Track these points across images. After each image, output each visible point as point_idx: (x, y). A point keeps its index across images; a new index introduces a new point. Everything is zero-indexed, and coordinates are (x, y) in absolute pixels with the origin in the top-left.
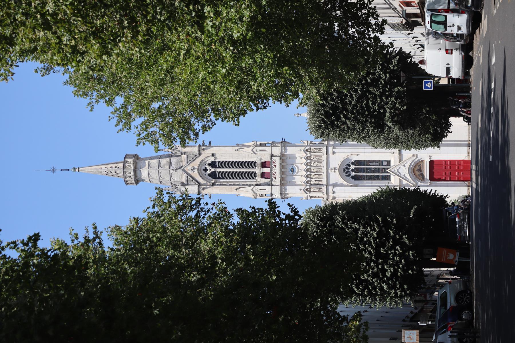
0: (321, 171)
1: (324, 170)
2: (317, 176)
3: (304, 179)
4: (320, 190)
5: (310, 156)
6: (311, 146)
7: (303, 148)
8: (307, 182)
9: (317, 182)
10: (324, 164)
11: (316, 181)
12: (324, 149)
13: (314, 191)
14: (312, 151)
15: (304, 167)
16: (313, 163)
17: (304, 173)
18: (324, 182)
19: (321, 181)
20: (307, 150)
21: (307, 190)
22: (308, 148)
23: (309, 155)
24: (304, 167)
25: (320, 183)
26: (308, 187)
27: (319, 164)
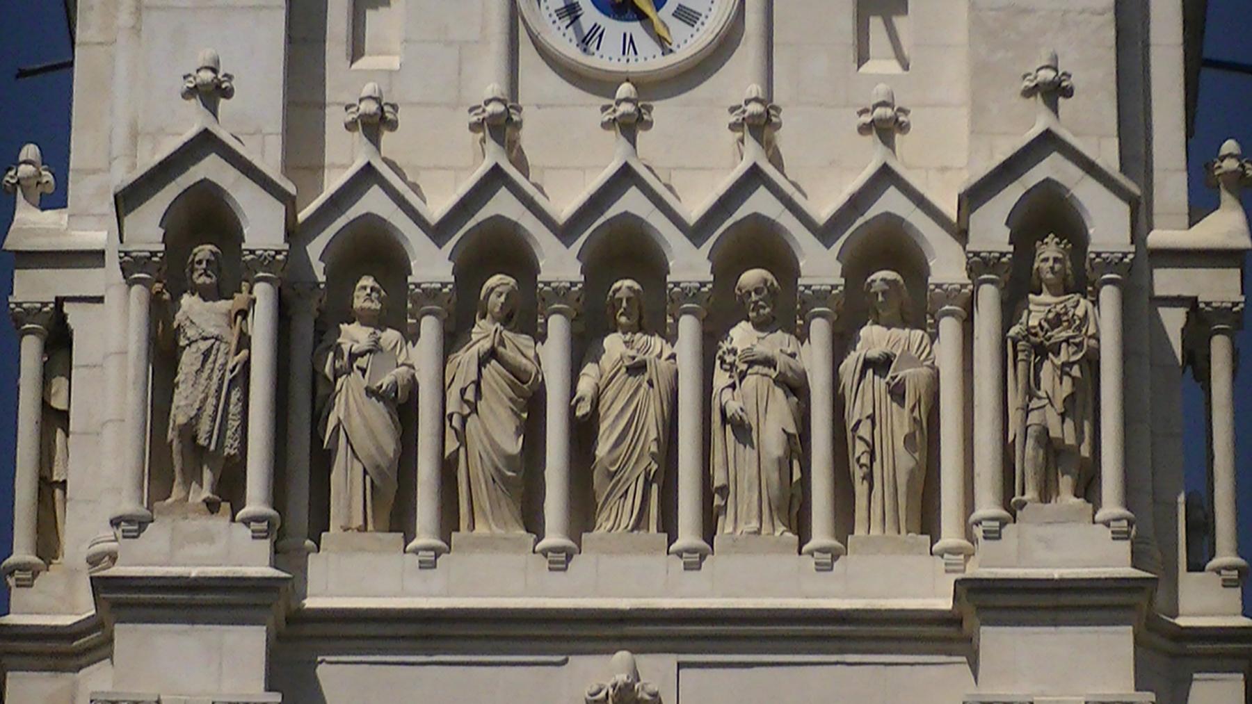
0: (615, 518)
1: (624, 573)
2: (498, 429)
3: (439, 169)
4: (181, 458)
5: (916, 308)
6: (1139, 308)
7: (1092, 124)
8: (375, 252)
9: (356, 414)
10: (757, 574)
11: (402, 406)
12: (1078, 543)
13: (163, 352)
14: (1039, 307)
15: (693, 160)
16: (776, 343)
17: (569, 163)
18: (351, 575)
19: (399, 519)
20: (1049, 215)
21: (206, 218)
22: (1107, 226)
23: (946, 266)
24: (693, 160)
25: (347, 487)
26: (262, 227)
27: (748, 472)
